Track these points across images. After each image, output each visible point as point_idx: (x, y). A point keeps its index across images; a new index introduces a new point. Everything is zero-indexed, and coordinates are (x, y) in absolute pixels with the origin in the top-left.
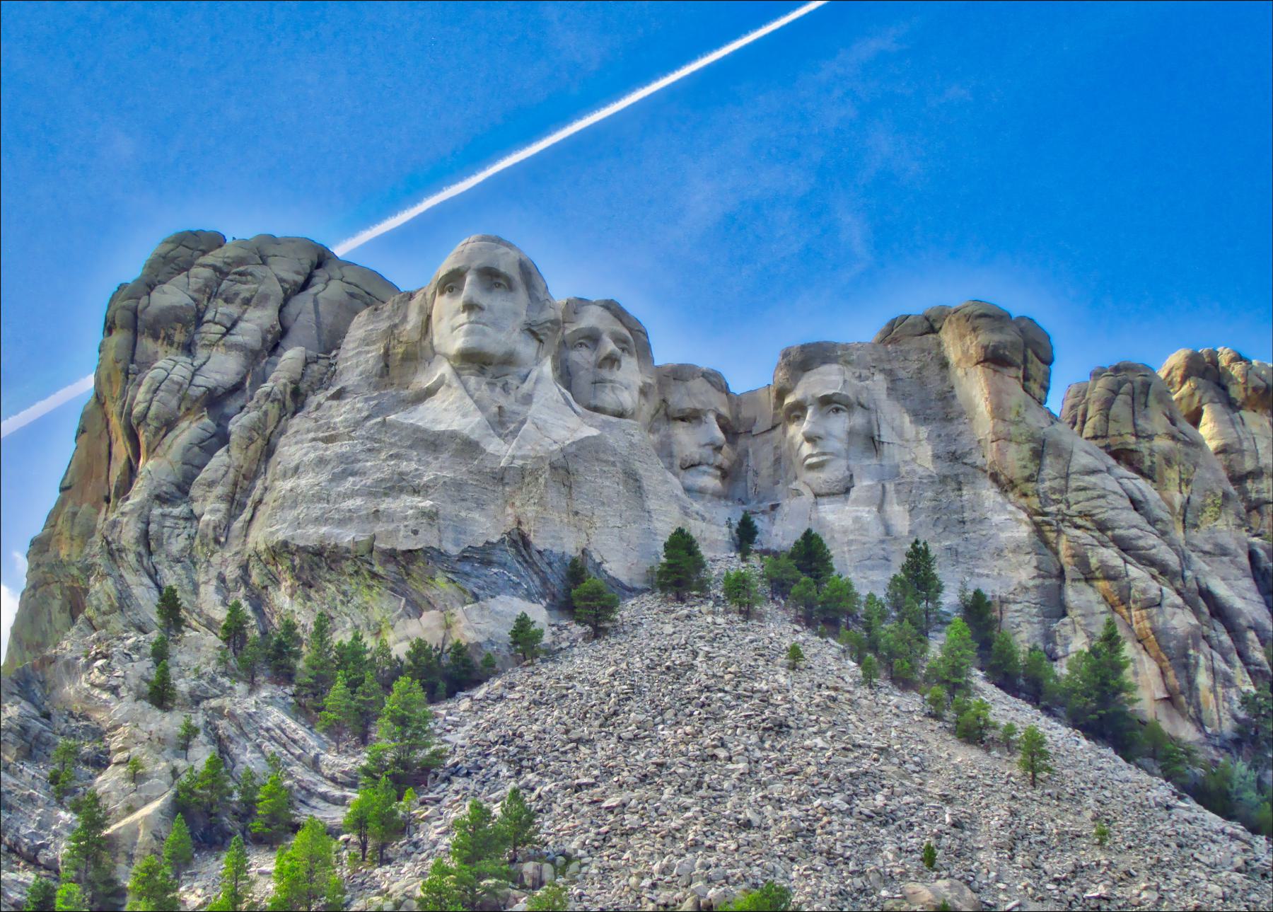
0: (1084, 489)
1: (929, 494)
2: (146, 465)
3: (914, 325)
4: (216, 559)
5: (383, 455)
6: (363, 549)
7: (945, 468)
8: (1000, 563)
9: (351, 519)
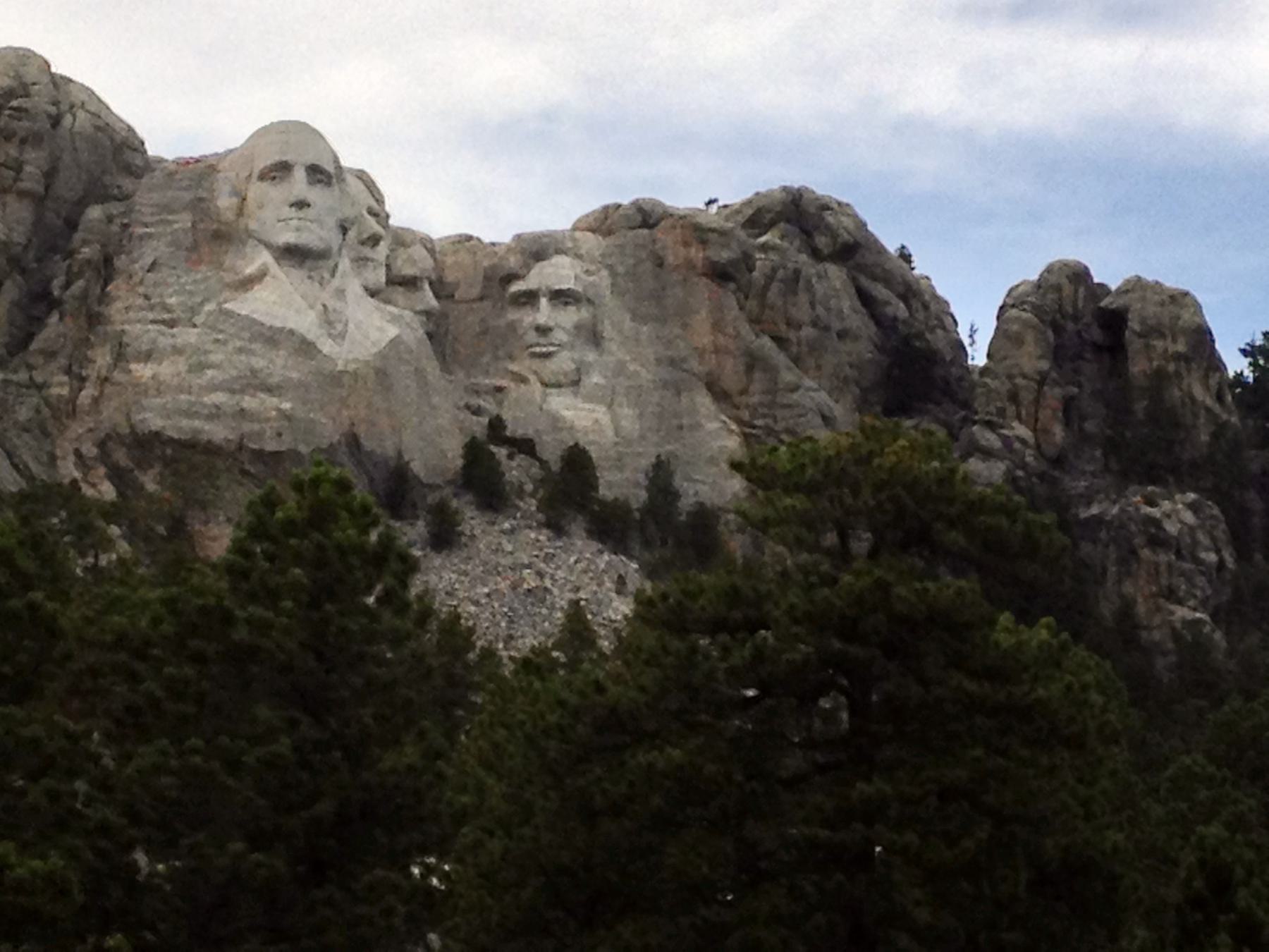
0: (789, 406)
3: (627, 217)
4: (70, 434)
5: (230, 347)
6: (233, 447)
7: (666, 373)
8: (714, 470)
9: (218, 417)
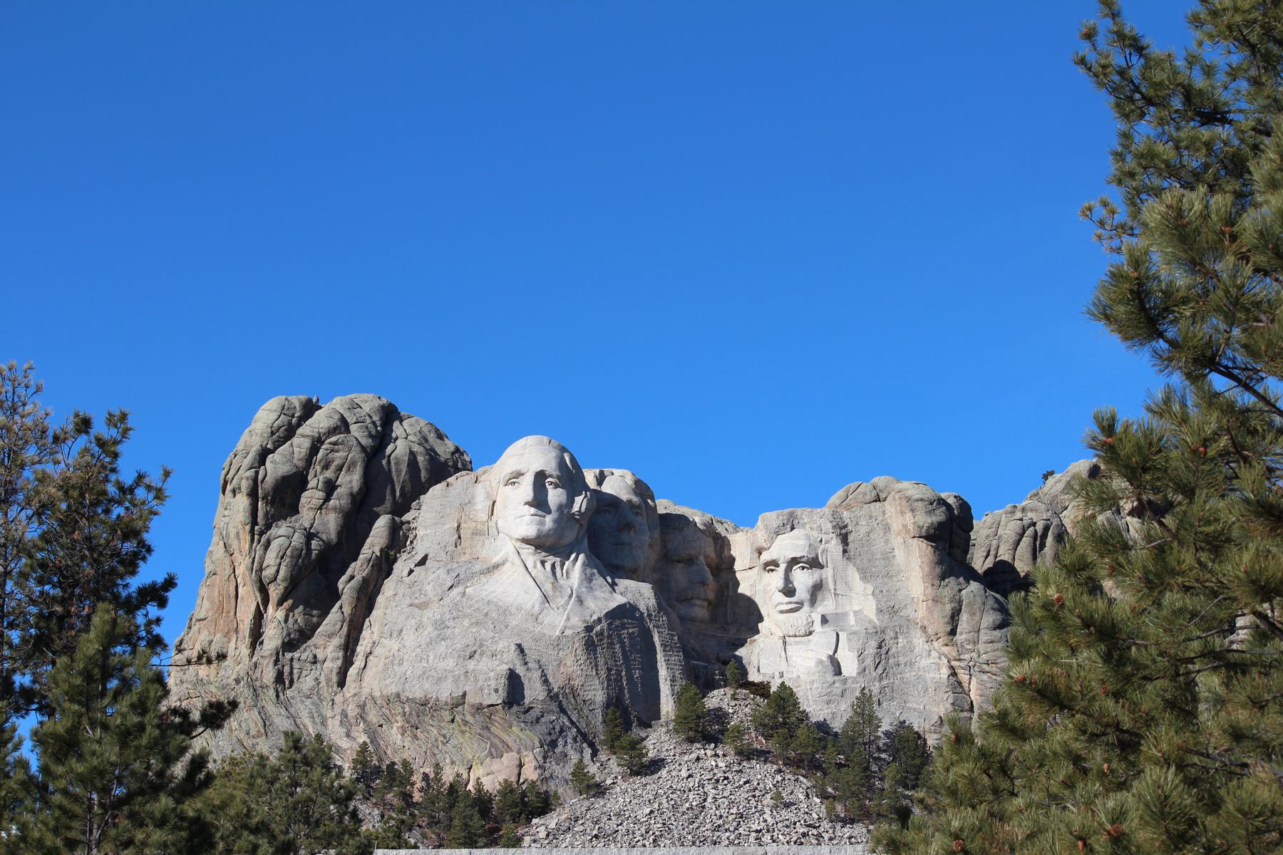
1: (873, 644)
2: (274, 614)
3: (865, 494)
